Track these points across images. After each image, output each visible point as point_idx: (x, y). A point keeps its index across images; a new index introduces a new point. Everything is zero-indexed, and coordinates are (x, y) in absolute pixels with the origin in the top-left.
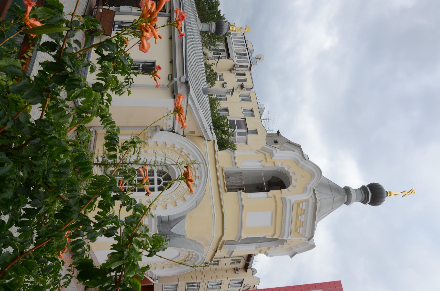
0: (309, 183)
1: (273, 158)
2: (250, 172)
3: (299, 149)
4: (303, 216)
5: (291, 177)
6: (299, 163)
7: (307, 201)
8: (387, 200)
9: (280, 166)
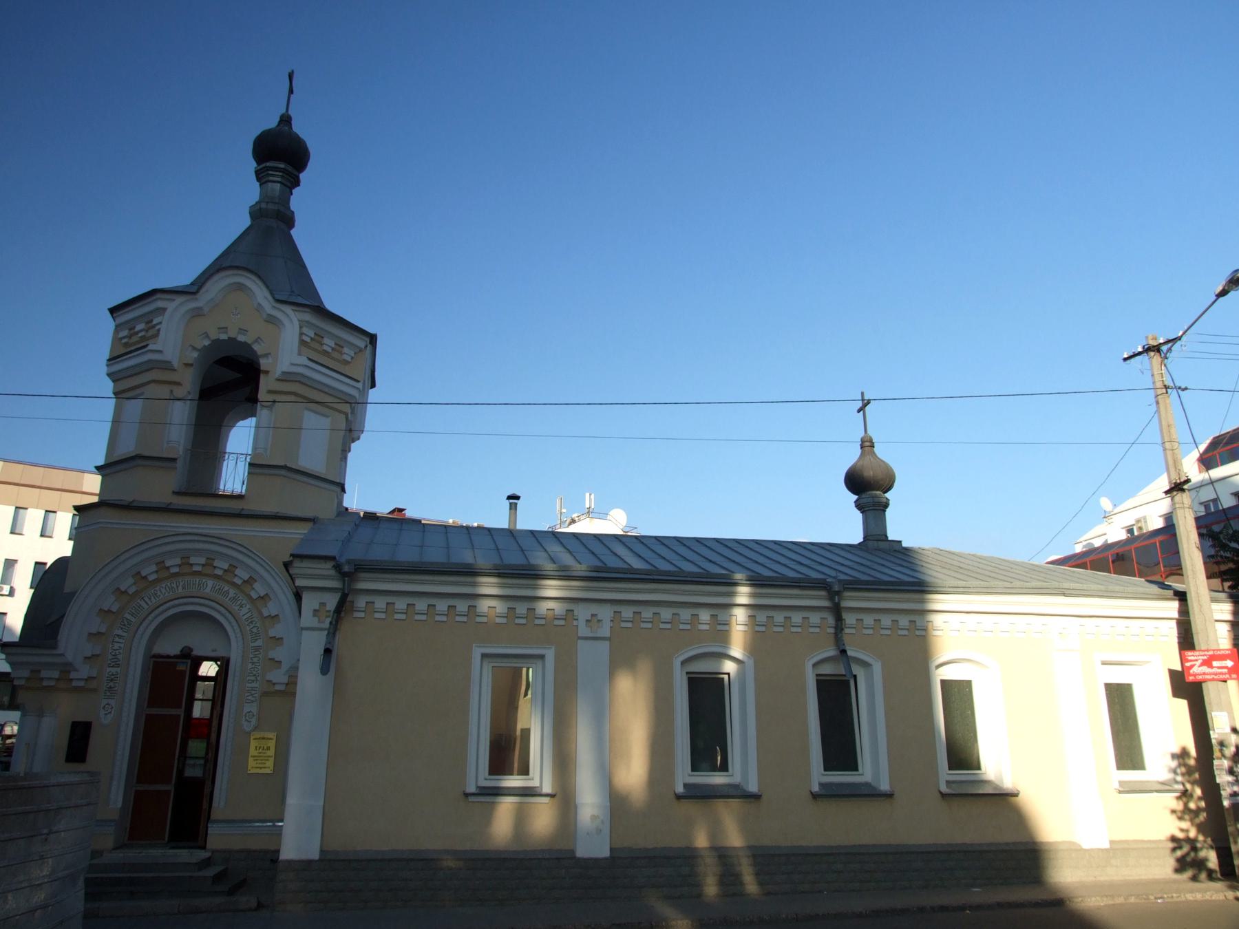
0: (259, 304)
1: (175, 364)
2: (227, 436)
3: (158, 296)
4: (346, 350)
5: (232, 340)
6: (200, 308)
7: (302, 324)
9: (195, 354)
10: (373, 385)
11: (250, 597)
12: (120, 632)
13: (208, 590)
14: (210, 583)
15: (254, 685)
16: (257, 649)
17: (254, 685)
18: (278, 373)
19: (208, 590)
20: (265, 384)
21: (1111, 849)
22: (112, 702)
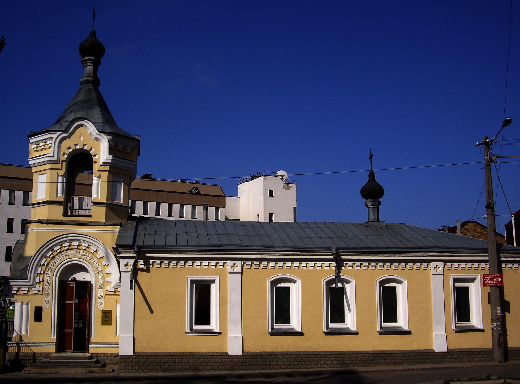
8: (100, 38)
10: (139, 154)
11: (97, 257)
12: (48, 272)
13: (80, 255)
14: (81, 252)
15: (101, 292)
16: (101, 278)
17: (101, 292)
18: (101, 163)
19: (80, 255)
20: (96, 167)
21: (448, 352)
22: (48, 299)
